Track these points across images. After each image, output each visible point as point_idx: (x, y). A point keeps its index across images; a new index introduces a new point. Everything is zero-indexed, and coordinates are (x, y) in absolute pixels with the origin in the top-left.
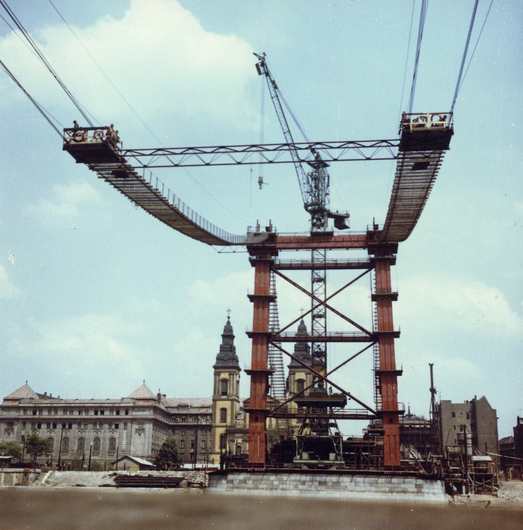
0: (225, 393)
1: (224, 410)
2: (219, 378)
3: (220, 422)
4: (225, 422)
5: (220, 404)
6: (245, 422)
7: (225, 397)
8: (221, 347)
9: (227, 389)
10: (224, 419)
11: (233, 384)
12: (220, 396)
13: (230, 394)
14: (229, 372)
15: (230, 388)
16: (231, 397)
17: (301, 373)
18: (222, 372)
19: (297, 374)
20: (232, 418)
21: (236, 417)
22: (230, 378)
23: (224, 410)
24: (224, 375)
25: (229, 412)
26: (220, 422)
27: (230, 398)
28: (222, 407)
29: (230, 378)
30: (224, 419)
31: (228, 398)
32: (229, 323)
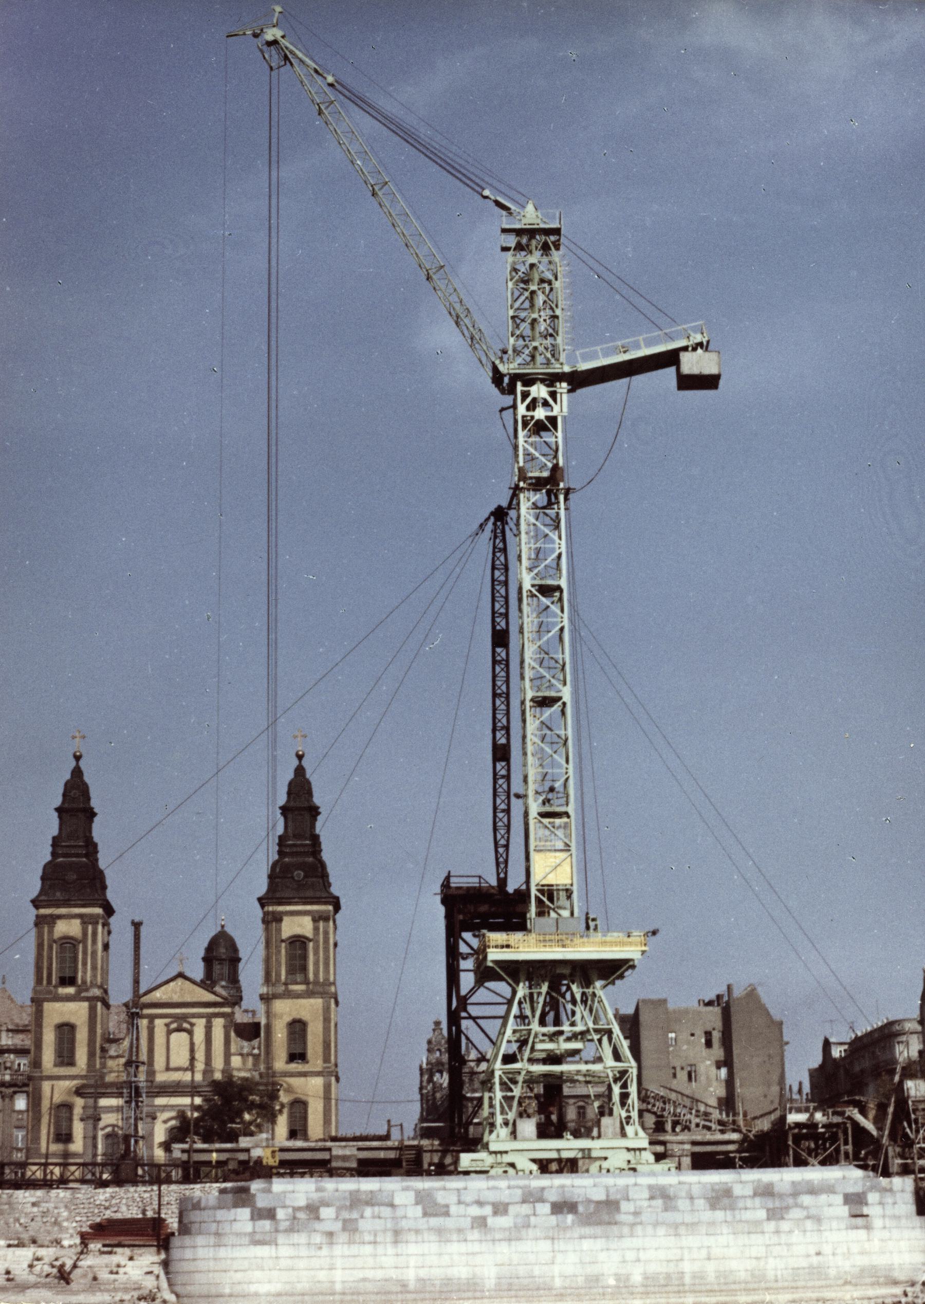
0: (68, 980)
1: (66, 1030)
2: (51, 932)
3: (55, 1065)
4: (71, 1063)
7: (71, 990)
9: (76, 971)
10: (65, 1057)
11: (94, 953)
12: (55, 987)
13: (84, 982)
14: (80, 916)
15: (85, 964)
16: (87, 990)
18: (60, 917)
19: (286, 920)
20: (91, 1055)
21: (103, 1050)
22: (85, 933)
23: (66, 1030)
24: (68, 928)
25: (82, 1036)
26: (55, 1065)
27: (83, 995)
28: (58, 1020)
29: (85, 933)
30: (65, 1057)
31: (79, 992)
32: (77, 773)
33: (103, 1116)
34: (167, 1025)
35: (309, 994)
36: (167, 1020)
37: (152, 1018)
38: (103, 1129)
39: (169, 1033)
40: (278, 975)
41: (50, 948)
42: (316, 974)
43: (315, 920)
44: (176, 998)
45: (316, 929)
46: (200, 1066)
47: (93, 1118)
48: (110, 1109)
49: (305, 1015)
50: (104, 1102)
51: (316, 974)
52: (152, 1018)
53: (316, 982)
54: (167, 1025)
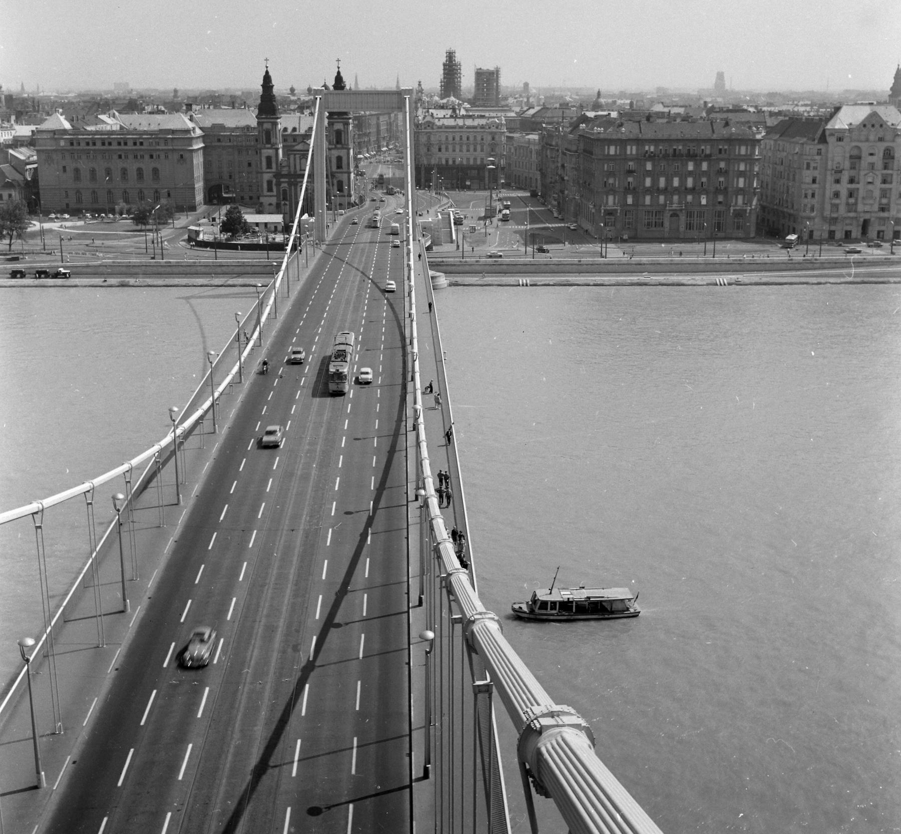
4: (271, 168)
6: (289, 168)
7: (269, 146)
8: (262, 96)
10: (269, 165)
17: (339, 124)
22: (273, 128)
25: (274, 159)
28: (267, 155)
29: (273, 128)
30: (269, 165)
32: (267, 72)
34: (300, 157)
35: (343, 148)
37: (295, 155)
39: (300, 159)
40: (333, 142)
42: (345, 142)
43: (344, 125)
44: (302, 149)
45: (344, 128)
47: (278, 184)
48: (283, 182)
49: (341, 154)
50: (282, 180)
51: (345, 142)
52: (295, 155)
53: (345, 144)
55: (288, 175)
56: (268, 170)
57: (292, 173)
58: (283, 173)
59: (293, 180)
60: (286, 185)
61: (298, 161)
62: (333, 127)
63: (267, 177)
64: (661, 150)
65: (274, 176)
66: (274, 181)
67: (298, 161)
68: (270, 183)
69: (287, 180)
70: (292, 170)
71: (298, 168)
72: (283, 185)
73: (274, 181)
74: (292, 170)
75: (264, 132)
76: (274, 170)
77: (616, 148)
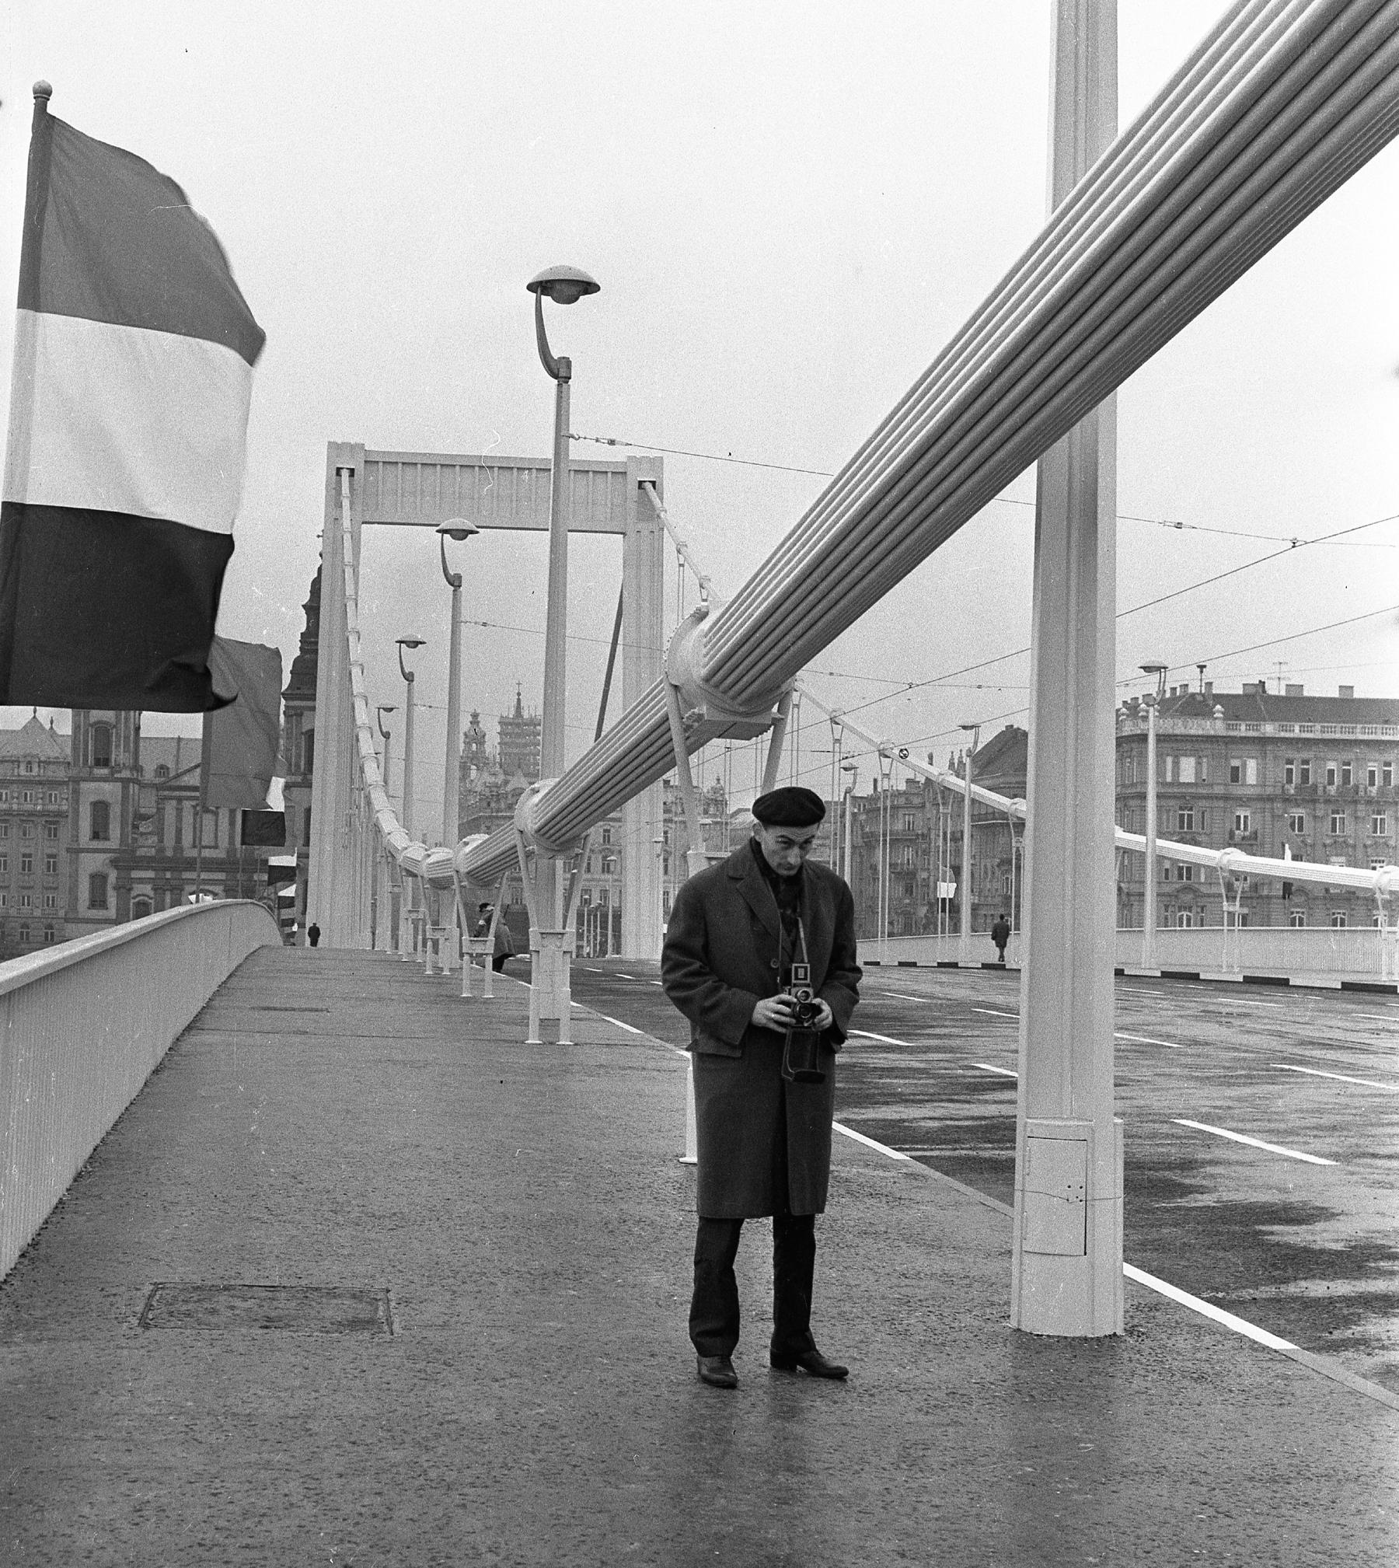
1: (100, 809)
5: (92, 791)
6: (161, 841)
7: (104, 771)
33: (135, 886)
34: (194, 807)
36: (194, 803)
37: (180, 800)
38: (134, 898)
40: (298, 766)
41: (87, 731)
46: (224, 842)
48: (141, 881)
52: (180, 800)
54: (194, 807)
55: (158, 862)
56: (95, 844)
57: (169, 853)
58: (141, 852)
59: (168, 875)
60: (147, 889)
61: (188, 818)
62: (299, 723)
63: (92, 863)
64: (1331, 772)
65: (114, 863)
66: (113, 876)
67: (188, 818)
68: (98, 881)
69: (151, 874)
70: (169, 841)
71: (187, 839)
72: (139, 889)
73: (113, 876)
74: (169, 841)
75: (91, 732)
76: (114, 843)
77: (1199, 763)
